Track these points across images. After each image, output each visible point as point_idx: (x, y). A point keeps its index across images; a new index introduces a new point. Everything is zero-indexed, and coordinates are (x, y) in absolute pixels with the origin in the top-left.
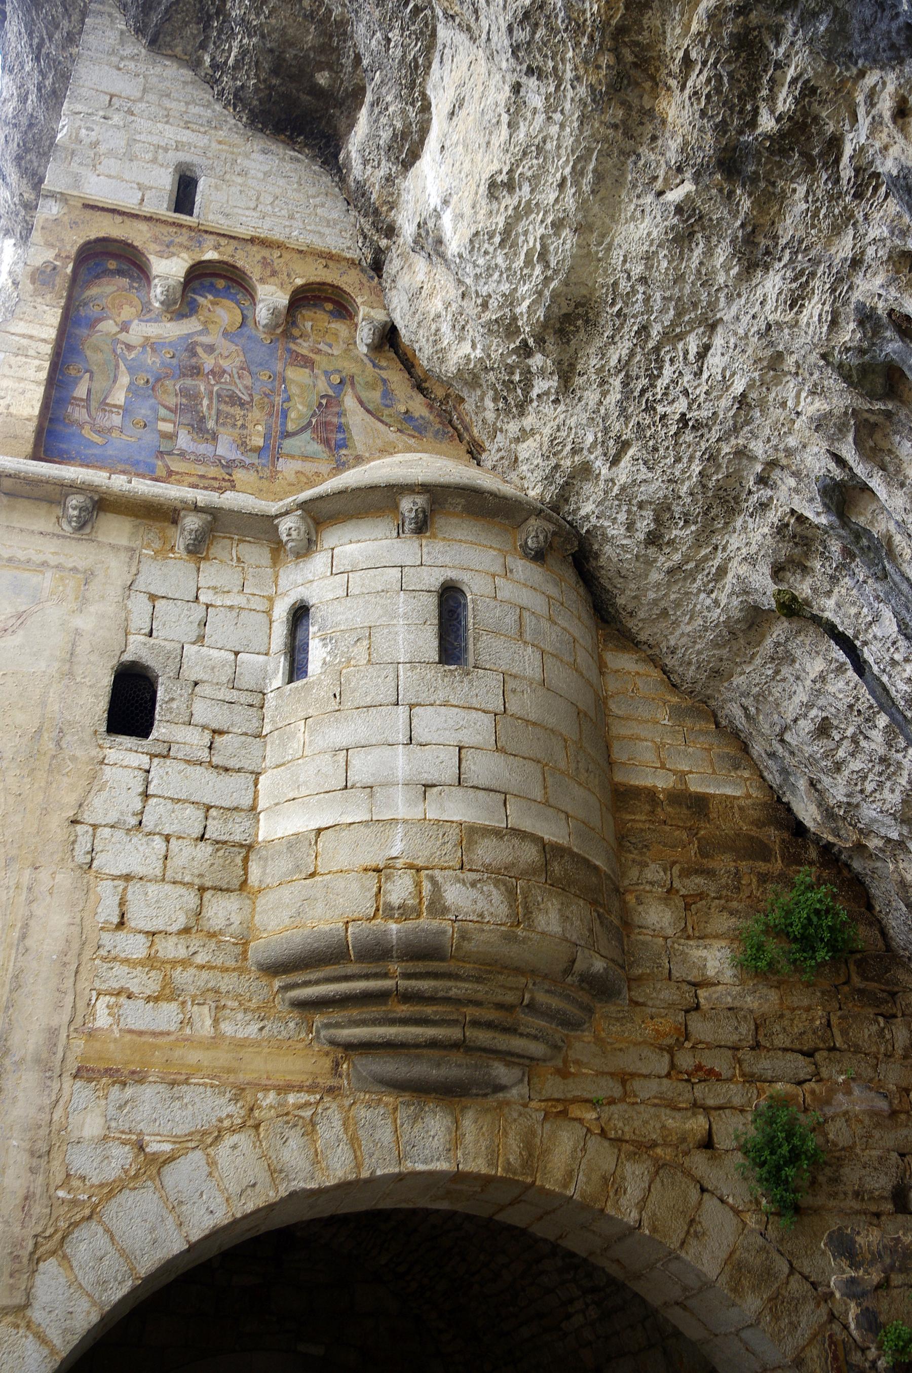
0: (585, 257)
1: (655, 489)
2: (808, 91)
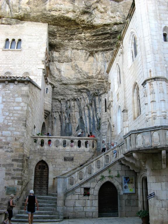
2: (84, 92)
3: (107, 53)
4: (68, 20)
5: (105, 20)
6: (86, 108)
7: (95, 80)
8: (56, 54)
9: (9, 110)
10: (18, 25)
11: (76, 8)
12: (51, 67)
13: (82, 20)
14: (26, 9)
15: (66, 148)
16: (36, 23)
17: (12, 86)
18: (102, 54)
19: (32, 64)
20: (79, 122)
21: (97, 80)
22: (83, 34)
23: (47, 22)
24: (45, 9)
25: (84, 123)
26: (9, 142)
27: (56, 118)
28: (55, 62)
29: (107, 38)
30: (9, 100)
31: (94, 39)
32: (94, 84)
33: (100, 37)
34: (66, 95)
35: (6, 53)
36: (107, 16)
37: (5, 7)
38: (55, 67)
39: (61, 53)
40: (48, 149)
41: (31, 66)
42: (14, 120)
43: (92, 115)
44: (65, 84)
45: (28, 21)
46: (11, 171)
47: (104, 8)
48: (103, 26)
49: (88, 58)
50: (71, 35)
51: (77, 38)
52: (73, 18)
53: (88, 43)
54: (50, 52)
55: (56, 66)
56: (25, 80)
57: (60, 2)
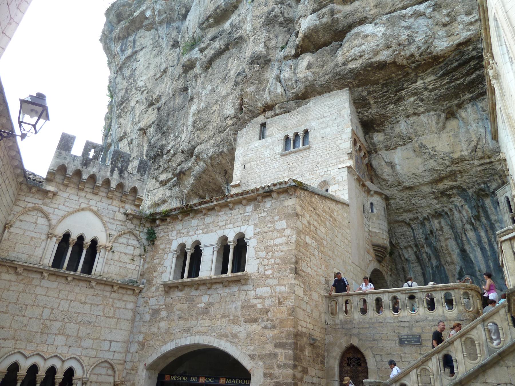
0: (418, 186)
1: (404, 206)
2: (453, 194)
3: (484, 99)
4: (382, 66)
5: (457, 34)
6: (468, 227)
7: (472, 162)
8: (378, 138)
9: (266, 247)
10: (300, 109)
11: (391, 39)
12: (374, 163)
13: (407, 56)
14: (306, 78)
15: (401, 315)
16: (328, 94)
17: (268, 204)
18: (473, 106)
19: (331, 165)
20: (459, 261)
21: (476, 162)
22: (419, 83)
23: (347, 86)
24: (337, 65)
25: (473, 259)
26: (268, 308)
27: (409, 259)
28: (380, 152)
29: (473, 68)
30: (265, 229)
31: (446, 81)
32: (472, 172)
33: (457, 74)
34: (417, 210)
35: (287, 159)
36: (459, 27)
37: (276, 88)
38: (382, 160)
39: (388, 131)
40: (361, 320)
41: (329, 169)
42: (275, 264)
43: (485, 240)
44: (410, 188)
45: (314, 96)
46: (272, 368)
47: (448, 15)
48: (455, 49)
49: (444, 125)
50: (397, 91)
51: (409, 94)
52: (389, 60)
53: (436, 95)
54: (367, 136)
55: (383, 159)
56: (287, 185)
57: (358, 42)
